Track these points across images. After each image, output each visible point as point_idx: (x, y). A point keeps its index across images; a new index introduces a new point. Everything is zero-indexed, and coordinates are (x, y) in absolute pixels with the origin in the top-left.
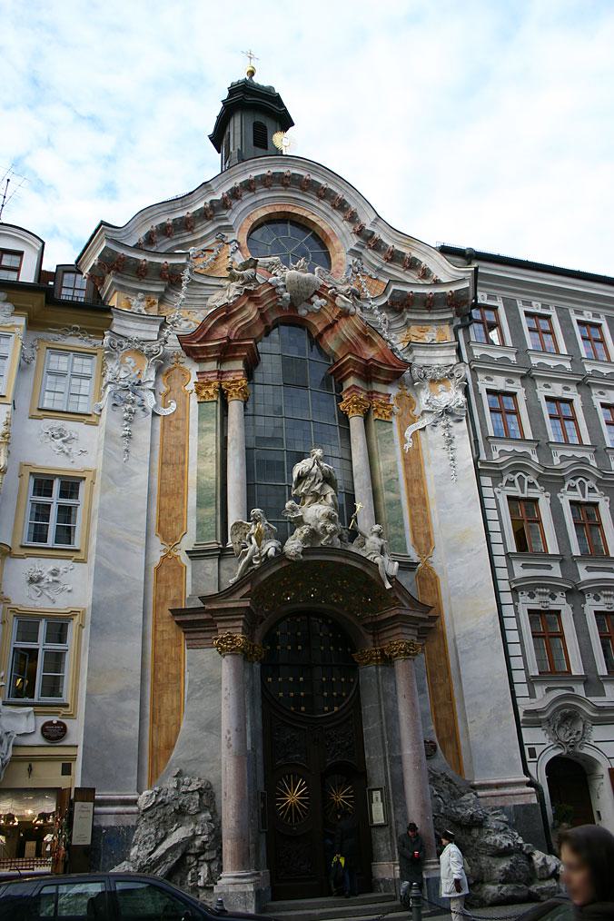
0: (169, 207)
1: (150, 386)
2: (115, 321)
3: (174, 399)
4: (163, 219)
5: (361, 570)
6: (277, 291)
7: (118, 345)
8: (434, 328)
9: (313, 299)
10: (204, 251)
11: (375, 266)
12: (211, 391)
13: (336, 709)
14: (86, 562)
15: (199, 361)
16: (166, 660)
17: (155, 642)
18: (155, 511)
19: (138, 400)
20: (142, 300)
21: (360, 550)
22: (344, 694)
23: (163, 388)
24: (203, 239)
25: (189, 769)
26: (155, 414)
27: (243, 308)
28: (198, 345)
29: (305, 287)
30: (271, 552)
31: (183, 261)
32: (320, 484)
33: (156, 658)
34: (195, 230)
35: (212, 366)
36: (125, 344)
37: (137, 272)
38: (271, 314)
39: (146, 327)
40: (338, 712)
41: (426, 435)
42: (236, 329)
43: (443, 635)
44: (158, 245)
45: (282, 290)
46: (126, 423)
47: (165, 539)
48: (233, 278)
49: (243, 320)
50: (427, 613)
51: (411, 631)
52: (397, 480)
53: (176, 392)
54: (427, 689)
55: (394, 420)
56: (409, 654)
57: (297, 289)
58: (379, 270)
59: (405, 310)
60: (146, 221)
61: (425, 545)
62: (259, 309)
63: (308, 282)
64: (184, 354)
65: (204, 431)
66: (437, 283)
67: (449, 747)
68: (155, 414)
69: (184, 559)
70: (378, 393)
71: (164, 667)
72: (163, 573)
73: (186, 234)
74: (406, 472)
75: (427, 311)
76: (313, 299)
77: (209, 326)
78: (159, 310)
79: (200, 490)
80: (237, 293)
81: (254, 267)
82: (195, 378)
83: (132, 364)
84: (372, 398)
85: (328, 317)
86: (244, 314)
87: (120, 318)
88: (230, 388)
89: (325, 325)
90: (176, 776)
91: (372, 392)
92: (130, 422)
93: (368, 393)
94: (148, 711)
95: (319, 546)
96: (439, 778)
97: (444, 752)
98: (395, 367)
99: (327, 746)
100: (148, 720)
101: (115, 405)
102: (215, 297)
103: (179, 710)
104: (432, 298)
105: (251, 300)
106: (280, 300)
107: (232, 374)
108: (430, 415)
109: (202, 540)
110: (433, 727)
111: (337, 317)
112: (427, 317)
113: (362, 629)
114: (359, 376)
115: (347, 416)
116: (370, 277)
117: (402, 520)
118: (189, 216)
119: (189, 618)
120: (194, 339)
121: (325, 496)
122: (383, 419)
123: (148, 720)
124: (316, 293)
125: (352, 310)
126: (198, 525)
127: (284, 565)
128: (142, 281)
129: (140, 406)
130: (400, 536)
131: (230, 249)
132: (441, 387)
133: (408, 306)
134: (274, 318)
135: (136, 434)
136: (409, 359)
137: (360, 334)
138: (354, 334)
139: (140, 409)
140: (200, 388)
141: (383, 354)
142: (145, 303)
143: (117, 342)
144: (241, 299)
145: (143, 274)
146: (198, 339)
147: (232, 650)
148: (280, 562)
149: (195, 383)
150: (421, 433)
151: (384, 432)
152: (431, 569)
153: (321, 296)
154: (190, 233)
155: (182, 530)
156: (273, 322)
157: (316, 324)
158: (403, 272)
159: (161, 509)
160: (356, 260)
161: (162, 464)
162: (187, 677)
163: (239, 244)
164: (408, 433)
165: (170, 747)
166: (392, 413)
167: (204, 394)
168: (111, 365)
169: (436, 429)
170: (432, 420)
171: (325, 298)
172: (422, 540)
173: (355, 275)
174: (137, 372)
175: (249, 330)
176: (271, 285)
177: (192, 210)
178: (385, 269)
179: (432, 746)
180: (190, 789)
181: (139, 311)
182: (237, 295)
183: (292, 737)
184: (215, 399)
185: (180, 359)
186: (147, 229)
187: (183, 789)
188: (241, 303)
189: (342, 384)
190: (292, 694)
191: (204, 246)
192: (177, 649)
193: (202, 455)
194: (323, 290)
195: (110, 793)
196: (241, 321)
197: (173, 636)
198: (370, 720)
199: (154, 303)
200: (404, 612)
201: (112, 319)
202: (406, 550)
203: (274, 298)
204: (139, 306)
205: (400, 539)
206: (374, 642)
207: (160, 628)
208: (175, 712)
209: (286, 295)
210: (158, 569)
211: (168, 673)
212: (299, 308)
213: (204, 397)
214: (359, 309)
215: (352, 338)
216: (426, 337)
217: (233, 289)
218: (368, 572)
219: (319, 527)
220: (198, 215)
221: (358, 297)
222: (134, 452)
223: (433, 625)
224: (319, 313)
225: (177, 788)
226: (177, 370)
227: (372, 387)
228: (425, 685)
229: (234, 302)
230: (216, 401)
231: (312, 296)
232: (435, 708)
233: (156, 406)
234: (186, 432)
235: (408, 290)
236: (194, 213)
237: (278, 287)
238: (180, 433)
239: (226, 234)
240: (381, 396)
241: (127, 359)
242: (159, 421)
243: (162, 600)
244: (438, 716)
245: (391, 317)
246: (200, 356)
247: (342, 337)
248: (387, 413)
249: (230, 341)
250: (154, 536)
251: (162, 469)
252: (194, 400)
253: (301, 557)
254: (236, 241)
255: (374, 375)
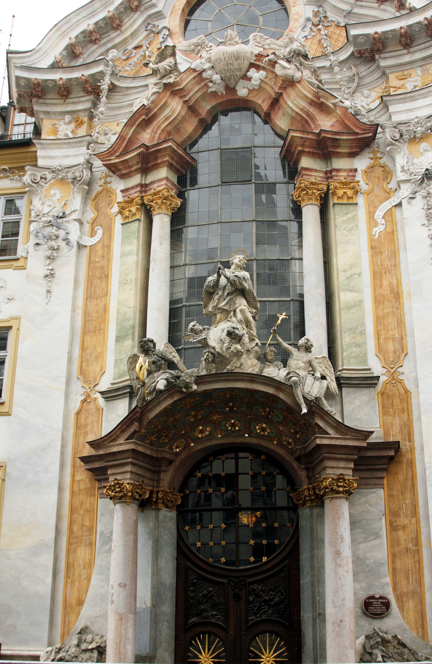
0: (88, 11)
1: (75, 216)
2: (40, 153)
3: (101, 226)
4: (83, 27)
5: (272, 395)
6: (204, 75)
7: (41, 178)
8: (419, 71)
9: (249, 74)
10: (136, 48)
11: (343, 10)
12: (133, 209)
13: (265, 559)
14: (10, 415)
15: (123, 177)
16: (81, 512)
17: (73, 493)
18: (77, 351)
19: (62, 233)
20: (70, 122)
21: (318, 364)
22: (276, 542)
23: (90, 215)
24: (133, 35)
25: (95, 628)
26: (80, 247)
27: (165, 105)
28: (117, 161)
29: (235, 62)
30: (161, 385)
31: (101, 68)
32: (229, 297)
33: (72, 510)
34: (123, 29)
35: (136, 179)
36: (49, 176)
37: (59, 93)
38: (203, 104)
39: (72, 151)
40: (266, 563)
41: (402, 211)
42: (159, 132)
43: (411, 464)
44: (85, 56)
45: (210, 72)
46: (48, 262)
47: (86, 381)
48: (155, 72)
49: (167, 119)
50: (365, 440)
51: (342, 464)
52: (359, 275)
53: (103, 216)
54: (384, 532)
55: (361, 200)
56: (338, 492)
57: (226, 68)
58: (350, 13)
59: (377, 56)
60: (63, 35)
61: (395, 352)
62: (185, 102)
63: (237, 57)
64: (111, 174)
65: (126, 255)
66: (412, 10)
67: (411, 604)
68: (80, 247)
69: (101, 401)
70: (338, 170)
71: (80, 519)
72: (82, 419)
73: (114, 35)
74: (373, 262)
75: (405, 51)
76: (249, 74)
77: (129, 136)
78: (90, 127)
79: (120, 323)
80: (155, 90)
81: (173, 54)
82: (120, 198)
83: (58, 196)
84: (331, 178)
85: (270, 91)
86: (167, 112)
87: (45, 149)
88: (152, 201)
89: (270, 101)
90: (80, 633)
91: (331, 171)
92: (53, 259)
93: (326, 173)
94: (63, 565)
95: (225, 371)
96: (388, 642)
97: (402, 608)
98: (357, 134)
99: (251, 603)
100: (62, 575)
101: (37, 244)
102: (139, 100)
103: (90, 565)
104: (406, 33)
105: (174, 93)
106: (210, 84)
107: (155, 186)
108: (408, 185)
109: (119, 377)
110: (388, 579)
111: (280, 88)
112: (407, 58)
113: (295, 464)
114: (312, 155)
115: (300, 206)
116: (338, 26)
117: (363, 324)
118: (111, 14)
119: (97, 465)
120: (112, 155)
121: (235, 311)
122: (345, 201)
123: (62, 575)
124: (252, 65)
125: (298, 75)
126: (116, 361)
127: (176, 398)
128: (67, 101)
129: (64, 240)
130: (358, 345)
131: (161, 36)
132: (424, 145)
133: (379, 51)
134: (208, 107)
135: (58, 273)
136: (382, 120)
137: (312, 103)
138: (303, 104)
139: (63, 244)
140: (123, 208)
141: (343, 121)
142: (73, 126)
143: (39, 175)
144: (162, 95)
145: (65, 93)
146: (118, 154)
147: (121, 498)
148: (171, 396)
149: (118, 203)
150: (397, 210)
151: (345, 218)
152: (401, 382)
153: (258, 68)
154: (118, 32)
155: (102, 370)
156: (209, 112)
157: (260, 102)
158: (378, 8)
159: (83, 349)
160: (316, 9)
161: (87, 299)
162: (99, 529)
163: (169, 30)
164: (379, 214)
165: (80, 603)
166: (356, 192)
167: (127, 213)
168: (37, 203)
169: (413, 201)
170: (410, 191)
171: (264, 69)
172: (391, 347)
173: (313, 28)
174: (63, 204)
175: (177, 129)
176: (194, 70)
177: (112, 8)
178: (356, 10)
179: (382, 603)
180: (90, 647)
181: (66, 135)
182: (154, 93)
183: (209, 592)
184: (138, 217)
185: (108, 179)
186: (65, 42)
187: (84, 646)
188: (161, 100)
189: (297, 168)
190: (265, 542)
191: (134, 44)
192: (92, 498)
193: (123, 283)
194: (259, 60)
195: (36, 649)
196: (163, 122)
197: (88, 485)
198: (305, 572)
199: (82, 123)
200: (326, 442)
201: (36, 152)
202: (365, 361)
203: (202, 84)
204: (67, 129)
205: (356, 350)
206: (309, 478)
207: (78, 477)
208: (87, 566)
209: (216, 78)
210: (78, 414)
211: (83, 525)
212: (237, 88)
213: (127, 217)
214: (307, 74)
215: (302, 110)
216: (408, 85)
217: (151, 87)
218: (281, 396)
219: (224, 349)
220: (122, 9)
221: (306, 57)
222: (55, 289)
223: (392, 453)
224: (260, 89)
225: (78, 645)
226: (104, 193)
227: (332, 166)
228: (381, 528)
229: (153, 102)
230: (139, 220)
231: (248, 71)
232: (394, 556)
233: (81, 237)
234: (109, 261)
235: (370, 30)
236: (117, 8)
237: (204, 70)
238: (104, 262)
239: (156, 23)
240: (344, 174)
241: (52, 192)
242: (86, 252)
243: (80, 448)
244: (398, 565)
245: (363, 70)
246: (124, 172)
247: (289, 111)
248: (350, 193)
249: (147, 148)
250: (76, 379)
251: (86, 306)
252: (119, 220)
253: (195, 387)
254: (165, 28)
255: (330, 149)
